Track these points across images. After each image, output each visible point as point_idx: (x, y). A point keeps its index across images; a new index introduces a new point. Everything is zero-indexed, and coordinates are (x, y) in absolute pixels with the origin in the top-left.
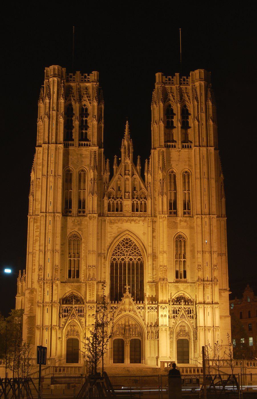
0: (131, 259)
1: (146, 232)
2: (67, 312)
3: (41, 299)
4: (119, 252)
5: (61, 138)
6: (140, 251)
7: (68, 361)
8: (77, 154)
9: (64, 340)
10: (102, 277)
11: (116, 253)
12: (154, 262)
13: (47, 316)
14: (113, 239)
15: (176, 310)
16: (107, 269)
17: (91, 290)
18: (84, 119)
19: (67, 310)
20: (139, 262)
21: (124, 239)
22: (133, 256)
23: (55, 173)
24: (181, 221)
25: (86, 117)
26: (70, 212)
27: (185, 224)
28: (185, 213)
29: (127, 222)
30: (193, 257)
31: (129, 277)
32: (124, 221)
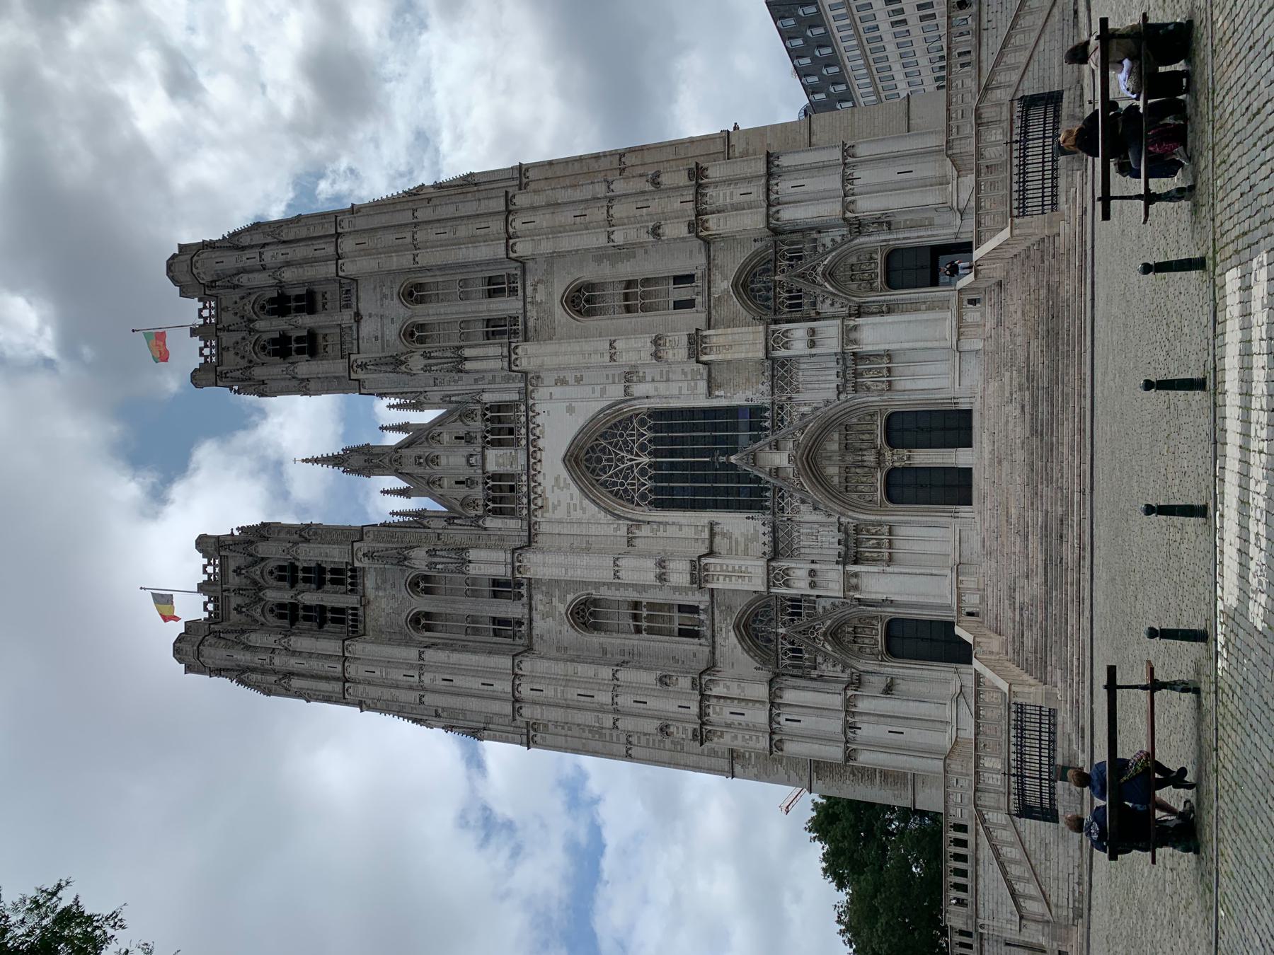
0: (643, 447)
1: (565, 404)
2: (800, 651)
3: (758, 738)
4: (622, 484)
5: (330, 646)
6: (620, 422)
8: (376, 597)
9: (895, 668)
10: (693, 536)
11: (626, 491)
12: (649, 378)
13: (809, 723)
14: (586, 502)
15: (790, 298)
16: (670, 521)
17: (726, 576)
18: (301, 575)
19: (793, 651)
20: (651, 422)
21: (588, 468)
22: (633, 441)
23: (412, 666)
24: (532, 303)
25: (294, 568)
26: (520, 623)
27: (541, 287)
28: (513, 291)
29: (540, 461)
30: (625, 251)
31: (694, 453)
32: (538, 469)
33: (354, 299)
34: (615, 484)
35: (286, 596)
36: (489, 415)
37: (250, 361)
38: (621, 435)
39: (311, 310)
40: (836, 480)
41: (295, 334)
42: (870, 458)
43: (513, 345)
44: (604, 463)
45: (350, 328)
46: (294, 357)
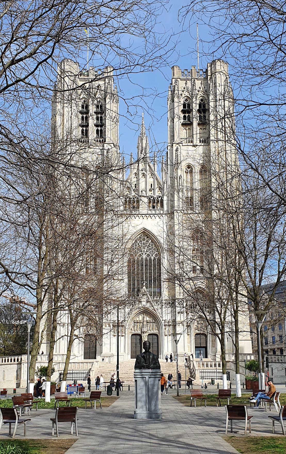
0: (148, 255)
7: (84, 359)
18: (99, 116)
33: (203, 144)
34: (136, 246)
35: (92, 109)
36: (160, 199)
37: (181, 95)
38: (152, 248)
39: (199, 124)
40: (138, 319)
41: (191, 115)
42: (145, 330)
43: (183, 211)
44: (143, 242)
45: (192, 142)
46: (182, 115)
